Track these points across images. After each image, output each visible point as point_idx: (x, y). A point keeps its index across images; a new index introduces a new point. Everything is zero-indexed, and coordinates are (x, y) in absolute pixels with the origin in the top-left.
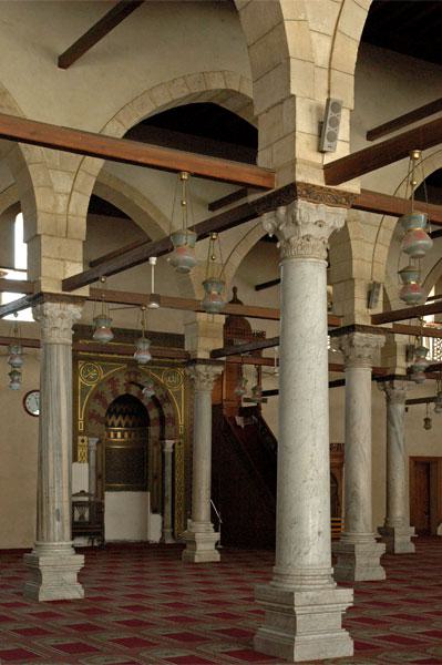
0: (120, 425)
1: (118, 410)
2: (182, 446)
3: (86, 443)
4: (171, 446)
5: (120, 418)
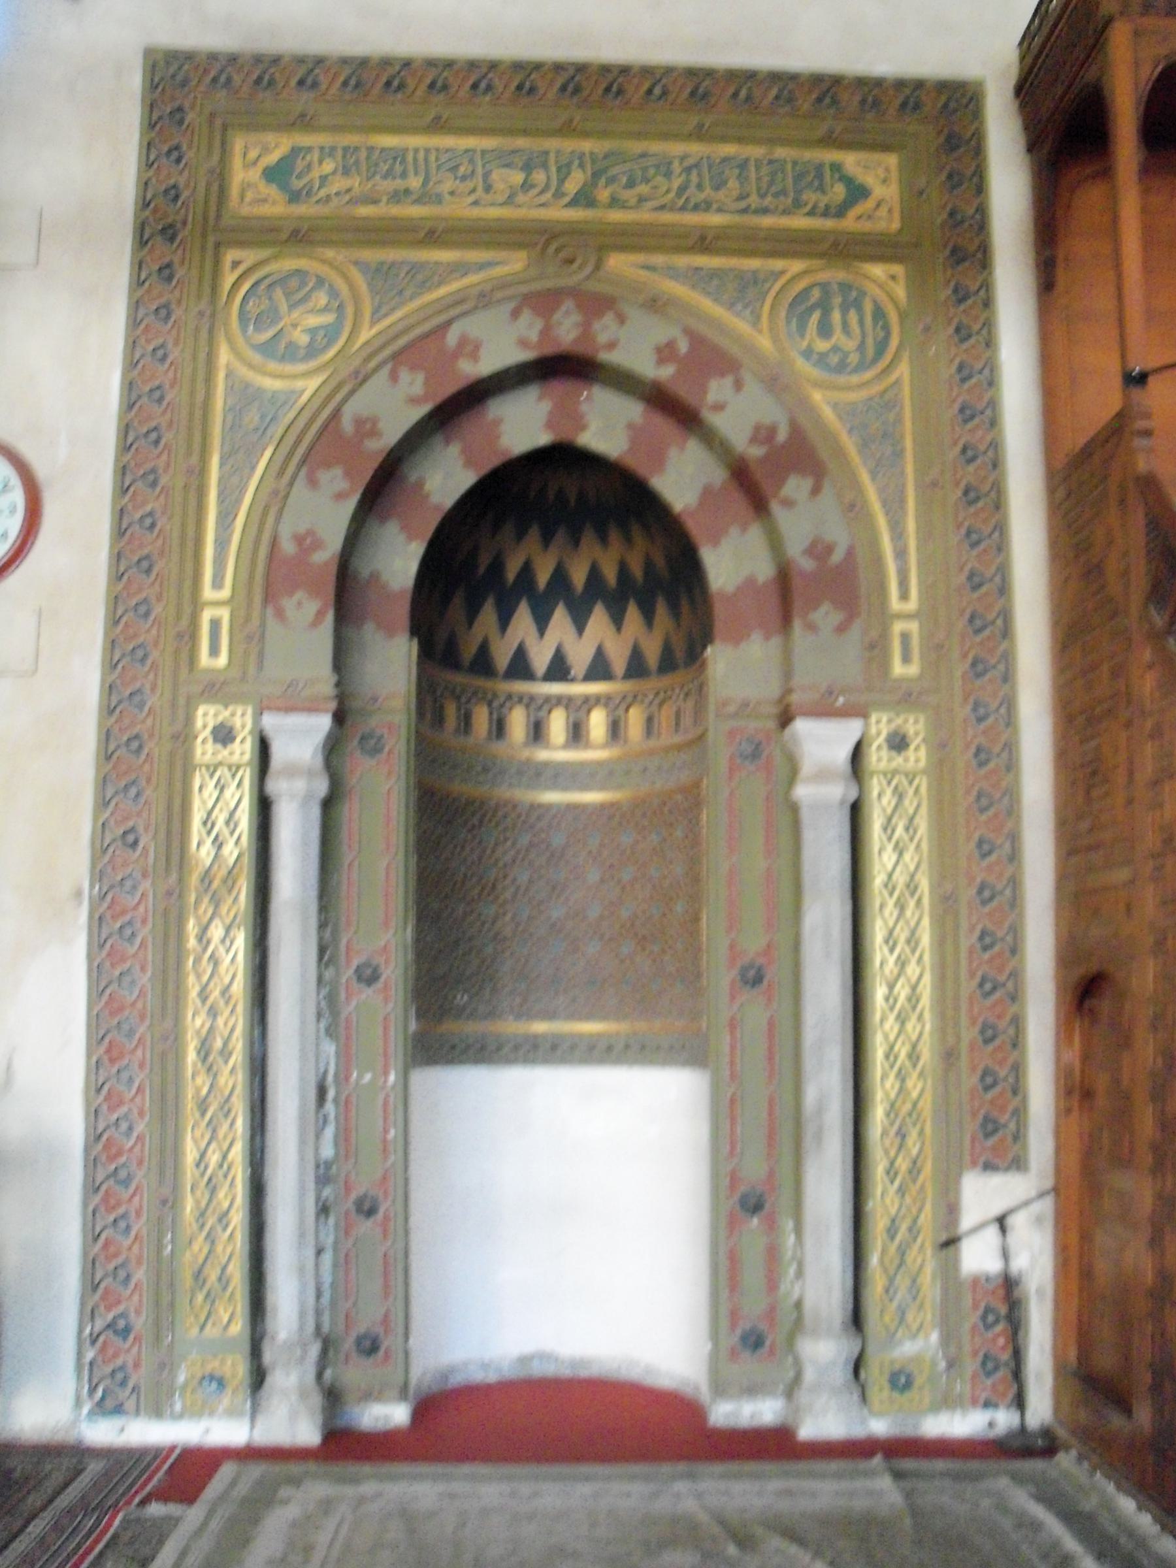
0: (599, 669)
1: (579, 577)
2: (917, 756)
3: (243, 750)
4: (843, 753)
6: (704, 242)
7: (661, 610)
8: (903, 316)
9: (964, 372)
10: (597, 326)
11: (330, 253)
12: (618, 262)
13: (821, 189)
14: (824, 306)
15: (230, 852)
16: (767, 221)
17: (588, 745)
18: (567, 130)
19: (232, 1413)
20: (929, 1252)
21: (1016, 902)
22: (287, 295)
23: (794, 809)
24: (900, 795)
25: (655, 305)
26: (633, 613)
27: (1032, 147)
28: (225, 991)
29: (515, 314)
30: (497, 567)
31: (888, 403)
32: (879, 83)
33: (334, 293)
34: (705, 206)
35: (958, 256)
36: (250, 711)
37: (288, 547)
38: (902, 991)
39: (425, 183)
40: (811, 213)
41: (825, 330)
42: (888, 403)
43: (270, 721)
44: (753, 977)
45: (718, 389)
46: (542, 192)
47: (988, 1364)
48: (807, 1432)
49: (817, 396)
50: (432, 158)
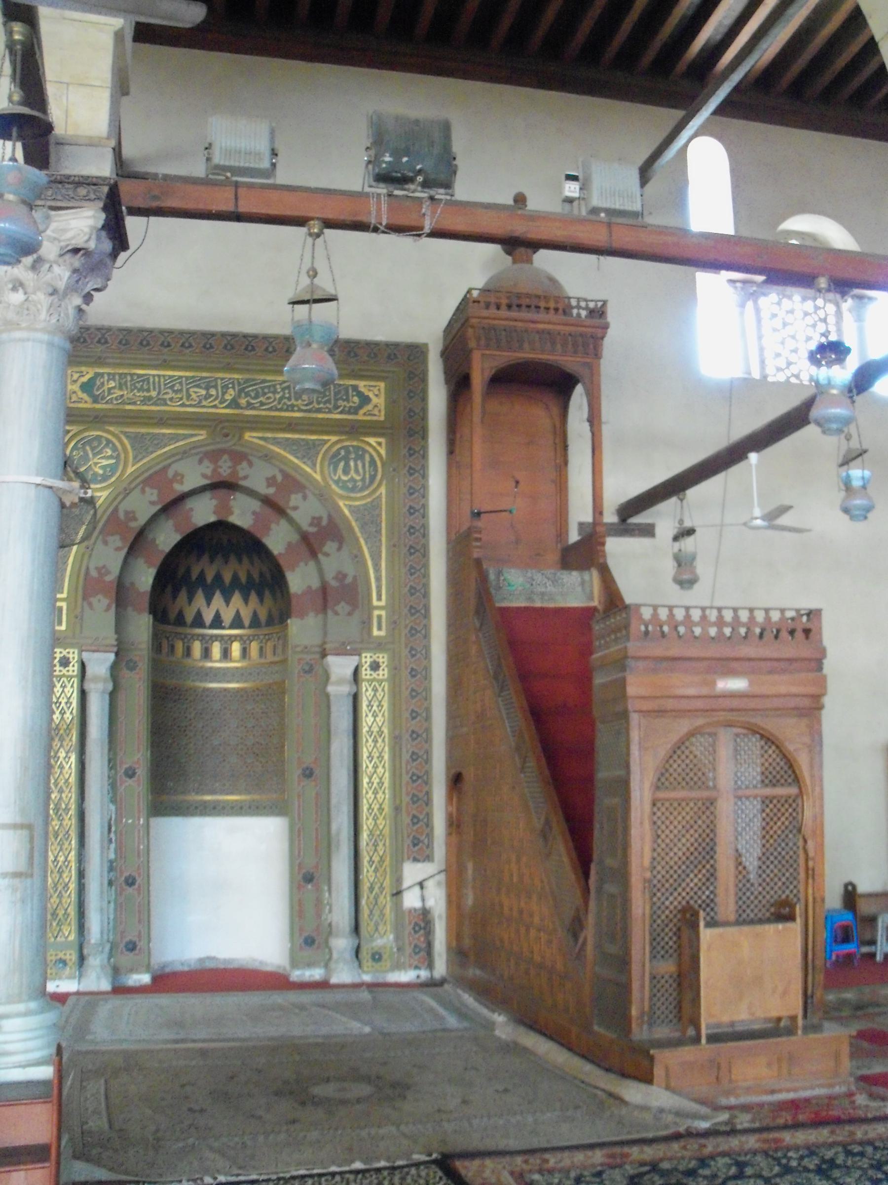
0: (237, 623)
1: (227, 577)
2: (383, 673)
3: (74, 669)
4: (349, 672)
5: (218, 600)
6: (291, 426)
7: (267, 594)
8: (383, 465)
9: (411, 491)
10: (239, 468)
11: (112, 429)
12: (249, 436)
13: (347, 400)
14: (346, 459)
15: (68, 716)
16: (320, 416)
17: (231, 660)
18: (229, 368)
19: (70, 977)
20: (388, 898)
21: (428, 740)
22: (93, 449)
23: (327, 696)
24: (375, 690)
25: (268, 457)
26: (253, 597)
27: (447, 381)
28: (67, 781)
29: (200, 461)
30: (188, 571)
31: (375, 506)
32: (377, 344)
33: (115, 449)
34: (291, 408)
35: (411, 433)
36: (76, 652)
37: (94, 573)
38: (376, 780)
39: (159, 393)
40: (341, 413)
41: (346, 471)
42: (375, 506)
43: (85, 655)
44: (308, 773)
45: (295, 499)
46: (215, 400)
47: (416, 950)
48: (334, 980)
49: (341, 503)
50: (162, 380)
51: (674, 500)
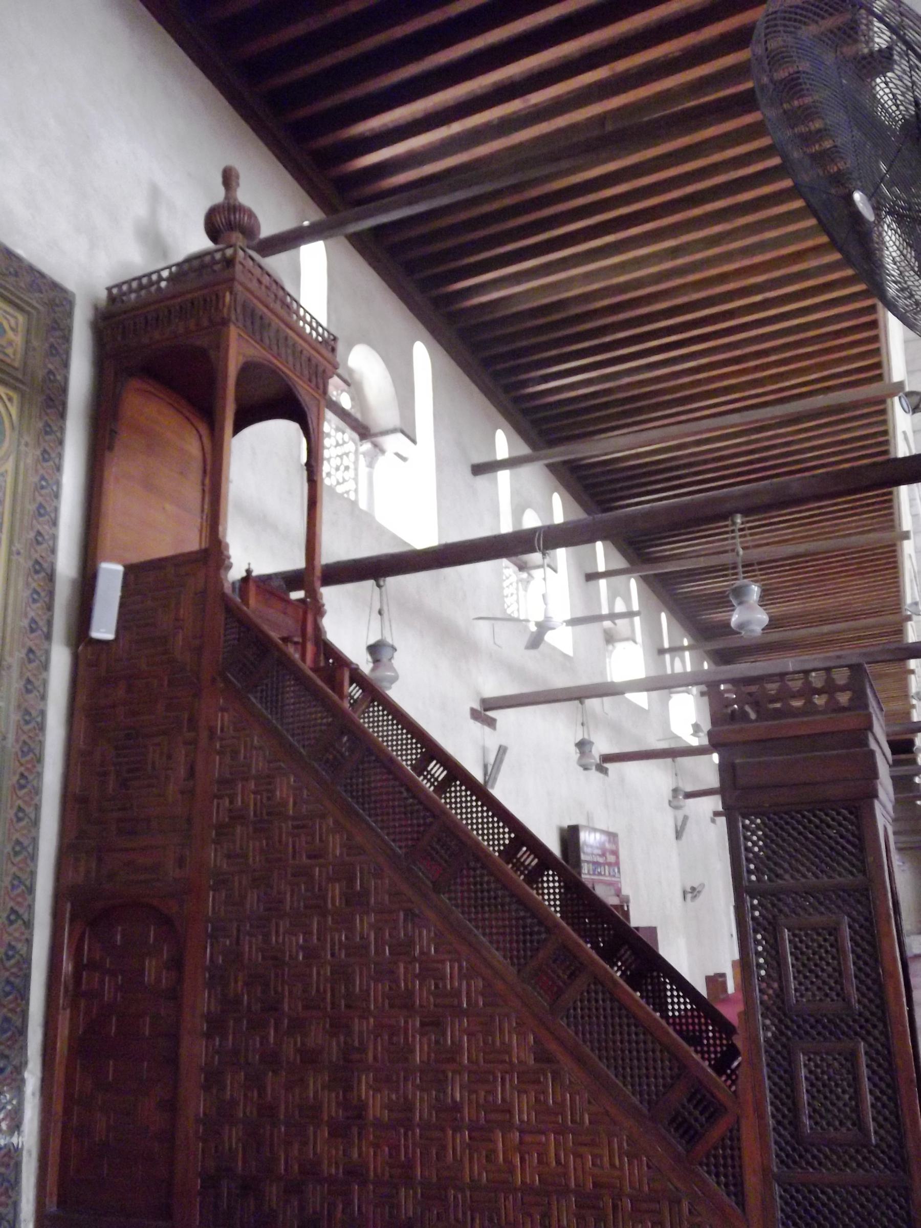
51: (370, 584)
